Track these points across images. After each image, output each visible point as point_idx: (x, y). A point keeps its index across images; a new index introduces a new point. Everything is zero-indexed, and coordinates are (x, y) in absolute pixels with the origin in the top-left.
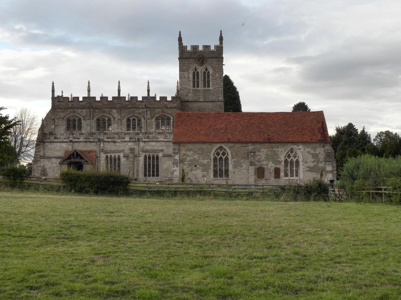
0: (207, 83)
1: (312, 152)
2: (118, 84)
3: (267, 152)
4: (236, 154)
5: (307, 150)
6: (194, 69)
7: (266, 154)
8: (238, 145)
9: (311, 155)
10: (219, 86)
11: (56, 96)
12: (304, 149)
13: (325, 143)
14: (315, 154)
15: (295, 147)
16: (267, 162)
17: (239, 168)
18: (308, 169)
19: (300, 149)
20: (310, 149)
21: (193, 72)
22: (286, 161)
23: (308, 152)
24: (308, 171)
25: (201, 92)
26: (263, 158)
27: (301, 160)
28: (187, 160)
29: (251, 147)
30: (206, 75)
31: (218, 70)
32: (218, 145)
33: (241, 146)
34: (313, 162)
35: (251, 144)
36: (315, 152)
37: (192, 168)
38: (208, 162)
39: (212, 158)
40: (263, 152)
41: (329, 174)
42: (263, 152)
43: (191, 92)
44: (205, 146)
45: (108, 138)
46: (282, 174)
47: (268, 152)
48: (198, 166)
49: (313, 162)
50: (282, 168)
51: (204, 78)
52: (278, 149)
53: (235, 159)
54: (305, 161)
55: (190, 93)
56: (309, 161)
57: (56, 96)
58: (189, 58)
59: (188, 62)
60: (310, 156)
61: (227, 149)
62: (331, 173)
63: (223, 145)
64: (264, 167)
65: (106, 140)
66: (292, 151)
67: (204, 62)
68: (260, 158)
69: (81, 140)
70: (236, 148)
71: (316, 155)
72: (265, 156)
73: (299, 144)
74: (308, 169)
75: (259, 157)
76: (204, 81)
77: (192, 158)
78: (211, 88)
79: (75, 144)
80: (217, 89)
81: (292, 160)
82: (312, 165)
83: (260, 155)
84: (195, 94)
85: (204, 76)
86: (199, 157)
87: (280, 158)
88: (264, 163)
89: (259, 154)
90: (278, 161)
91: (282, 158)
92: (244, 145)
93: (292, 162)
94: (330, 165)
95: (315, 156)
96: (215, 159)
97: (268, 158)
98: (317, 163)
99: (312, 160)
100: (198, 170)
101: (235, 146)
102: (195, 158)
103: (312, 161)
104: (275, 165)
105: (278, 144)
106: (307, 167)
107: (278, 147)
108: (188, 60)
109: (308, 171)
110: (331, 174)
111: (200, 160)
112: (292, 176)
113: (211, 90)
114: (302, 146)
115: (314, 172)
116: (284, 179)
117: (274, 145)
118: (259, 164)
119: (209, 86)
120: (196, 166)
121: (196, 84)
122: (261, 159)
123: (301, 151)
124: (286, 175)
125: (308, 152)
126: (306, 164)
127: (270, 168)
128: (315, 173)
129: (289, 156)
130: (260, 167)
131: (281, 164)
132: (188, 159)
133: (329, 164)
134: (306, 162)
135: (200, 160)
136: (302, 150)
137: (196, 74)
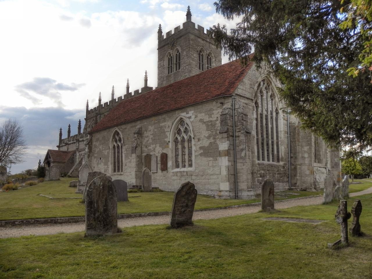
0: (178, 65)
1: (206, 119)
2: (112, 89)
3: (154, 131)
4: (127, 138)
5: (201, 116)
6: (169, 55)
7: (152, 134)
8: (129, 126)
9: (204, 125)
10: (186, 65)
11: (89, 109)
12: (196, 117)
13: (224, 98)
14: (211, 121)
15: (183, 115)
16: (154, 146)
17: (130, 157)
18: (202, 151)
19: (190, 118)
20: (203, 114)
21: (168, 58)
22: (176, 141)
23: (201, 121)
24: (201, 155)
25: (172, 76)
26: (150, 141)
27: (192, 136)
28: (96, 152)
29: (139, 125)
30: (179, 57)
31: (185, 48)
32: (113, 130)
33: (132, 127)
34: (208, 138)
35: (139, 122)
36: (211, 119)
37: (98, 161)
38: (108, 153)
39: (111, 146)
40: (150, 131)
41: (223, 158)
42: (150, 128)
43: (165, 79)
44: (105, 133)
45: (81, 138)
46: (170, 164)
47: (156, 130)
48: (102, 159)
49: (208, 138)
50: (170, 151)
51: (176, 61)
52: (166, 123)
53: (127, 146)
54: (198, 137)
55: (164, 81)
56: (203, 136)
57: (89, 109)
58: (164, 46)
59: (164, 50)
60: (204, 127)
61: (120, 133)
62: (225, 156)
63: (117, 129)
64: (151, 153)
65: (81, 139)
66: (182, 121)
67: (175, 44)
68: (147, 141)
69: (72, 142)
70: (127, 130)
71: (211, 124)
72: (152, 136)
73: (188, 109)
74: (202, 151)
75: (146, 139)
76: (176, 64)
77: (99, 149)
78: (180, 70)
79: (70, 145)
80: (185, 68)
81: (183, 137)
82: (206, 143)
83: (148, 136)
84: (168, 80)
85: (176, 59)
86: (103, 148)
87: (167, 137)
88: (151, 147)
89: (146, 135)
90: (165, 141)
91: (170, 137)
92: (133, 124)
93: (183, 140)
94: (223, 140)
95: (210, 125)
96: (114, 147)
97: (155, 139)
98: (214, 139)
99: (206, 134)
100: (102, 163)
101: (126, 128)
102: (100, 149)
103: (207, 136)
104: (163, 149)
105: (164, 116)
106: (201, 148)
107: (165, 121)
108: (163, 48)
109: (201, 155)
110: (227, 157)
111: (103, 151)
112: (184, 166)
113: (180, 71)
114: (193, 112)
115: (211, 157)
116: (172, 171)
117: (160, 117)
118: (146, 149)
119: (179, 69)
120: (100, 159)
121: (170, 69)
122: (149, 142)
123: (192, 120)
124: (177, 166)
125: (201, 121)
126: (199, 143)
127: (157, 155)
128: (211, 159)
129: (179, 132)
130: (147, 155)
131: (168, 147)
132: (97, 150)
133: (222, 138)
134: (199, 140)
135: (103, 151)
136: (193, 117)
137: (170, 60)
